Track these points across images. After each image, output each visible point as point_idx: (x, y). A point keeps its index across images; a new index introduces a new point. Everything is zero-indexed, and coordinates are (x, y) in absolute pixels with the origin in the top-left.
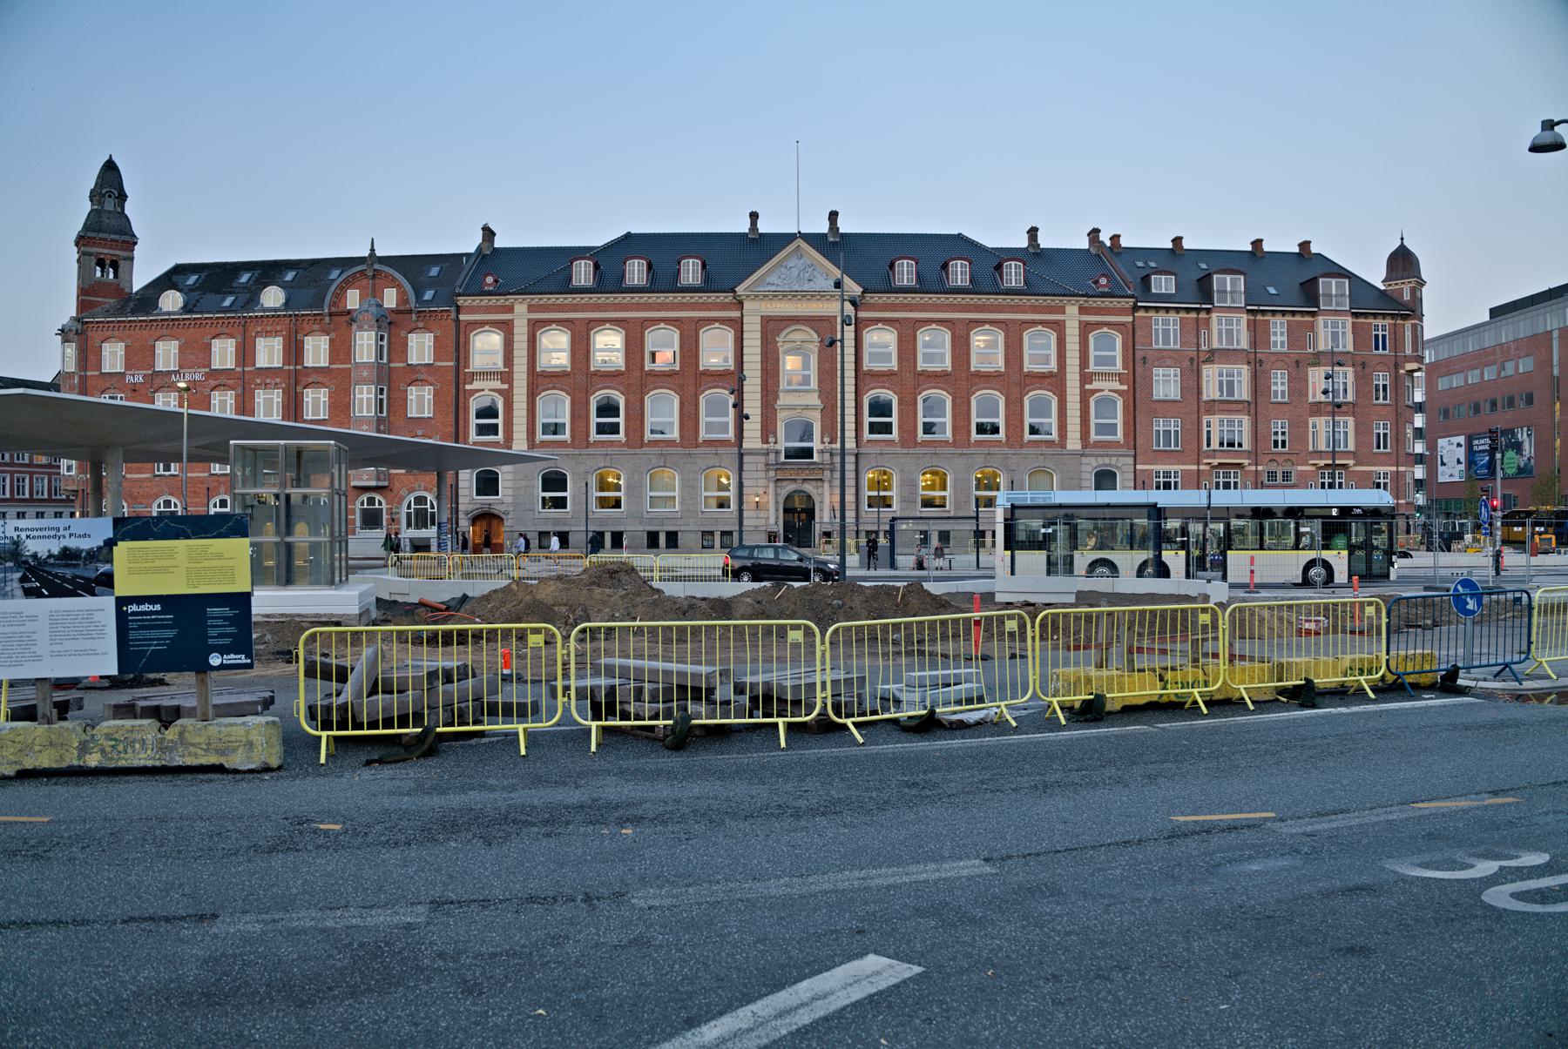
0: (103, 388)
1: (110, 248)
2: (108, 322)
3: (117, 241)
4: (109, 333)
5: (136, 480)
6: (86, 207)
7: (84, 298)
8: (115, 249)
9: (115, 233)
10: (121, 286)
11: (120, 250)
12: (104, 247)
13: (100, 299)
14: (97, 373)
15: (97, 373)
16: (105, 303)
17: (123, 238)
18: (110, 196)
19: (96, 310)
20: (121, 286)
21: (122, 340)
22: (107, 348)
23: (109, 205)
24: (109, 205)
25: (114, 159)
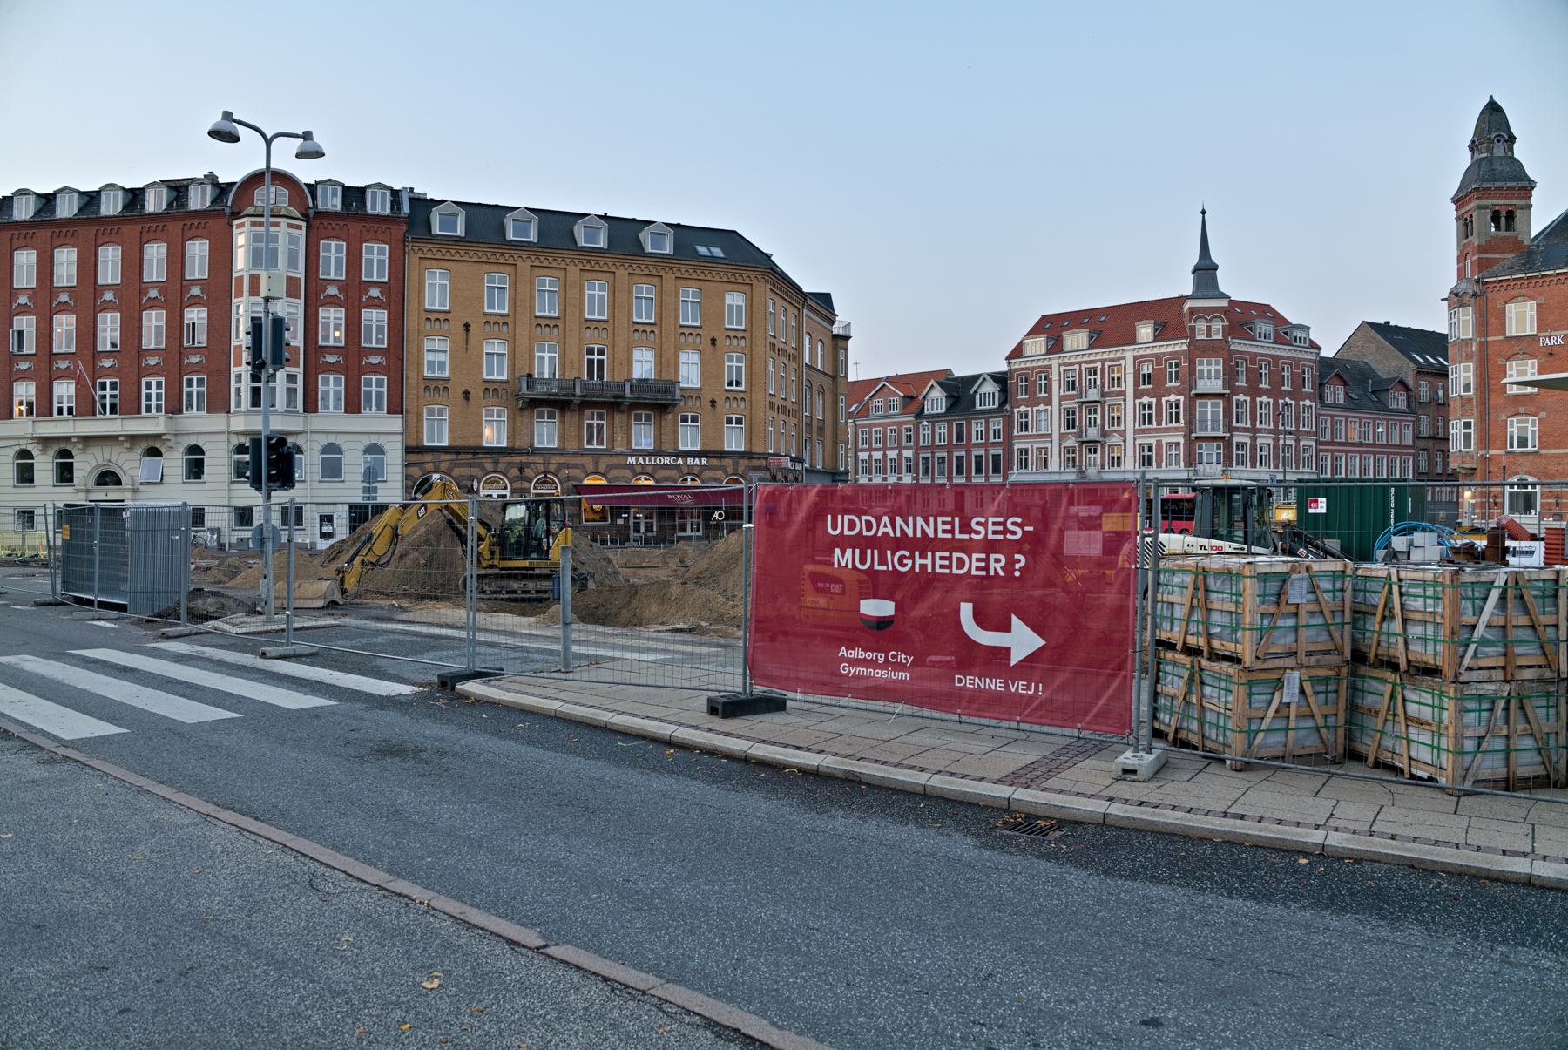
0: (1510, 353)
1: (1506, 198)
2: (1514, 279)
3: (1513, 189)
4: (1517, 292)
5: (1553, 456)
6: (1466, 159)
7: (1482, 256)
8: (1511, 198)
9: (1510, 180)
10: (1519, 239)
11: (1516, 198)
12: (1498, 198)
13: (1498, 256)
14: (1501, 338)
15: (1501, 338)
16: (1503, 259)
17: (1521, 184)
18: (1498, 141)
19: (1495, 268)
20: (1519, 239)
21: (1532, 298)
22: (1512, 310)
23: (1499, 151)
24: (1499, 151)
25: (1495, 99)
